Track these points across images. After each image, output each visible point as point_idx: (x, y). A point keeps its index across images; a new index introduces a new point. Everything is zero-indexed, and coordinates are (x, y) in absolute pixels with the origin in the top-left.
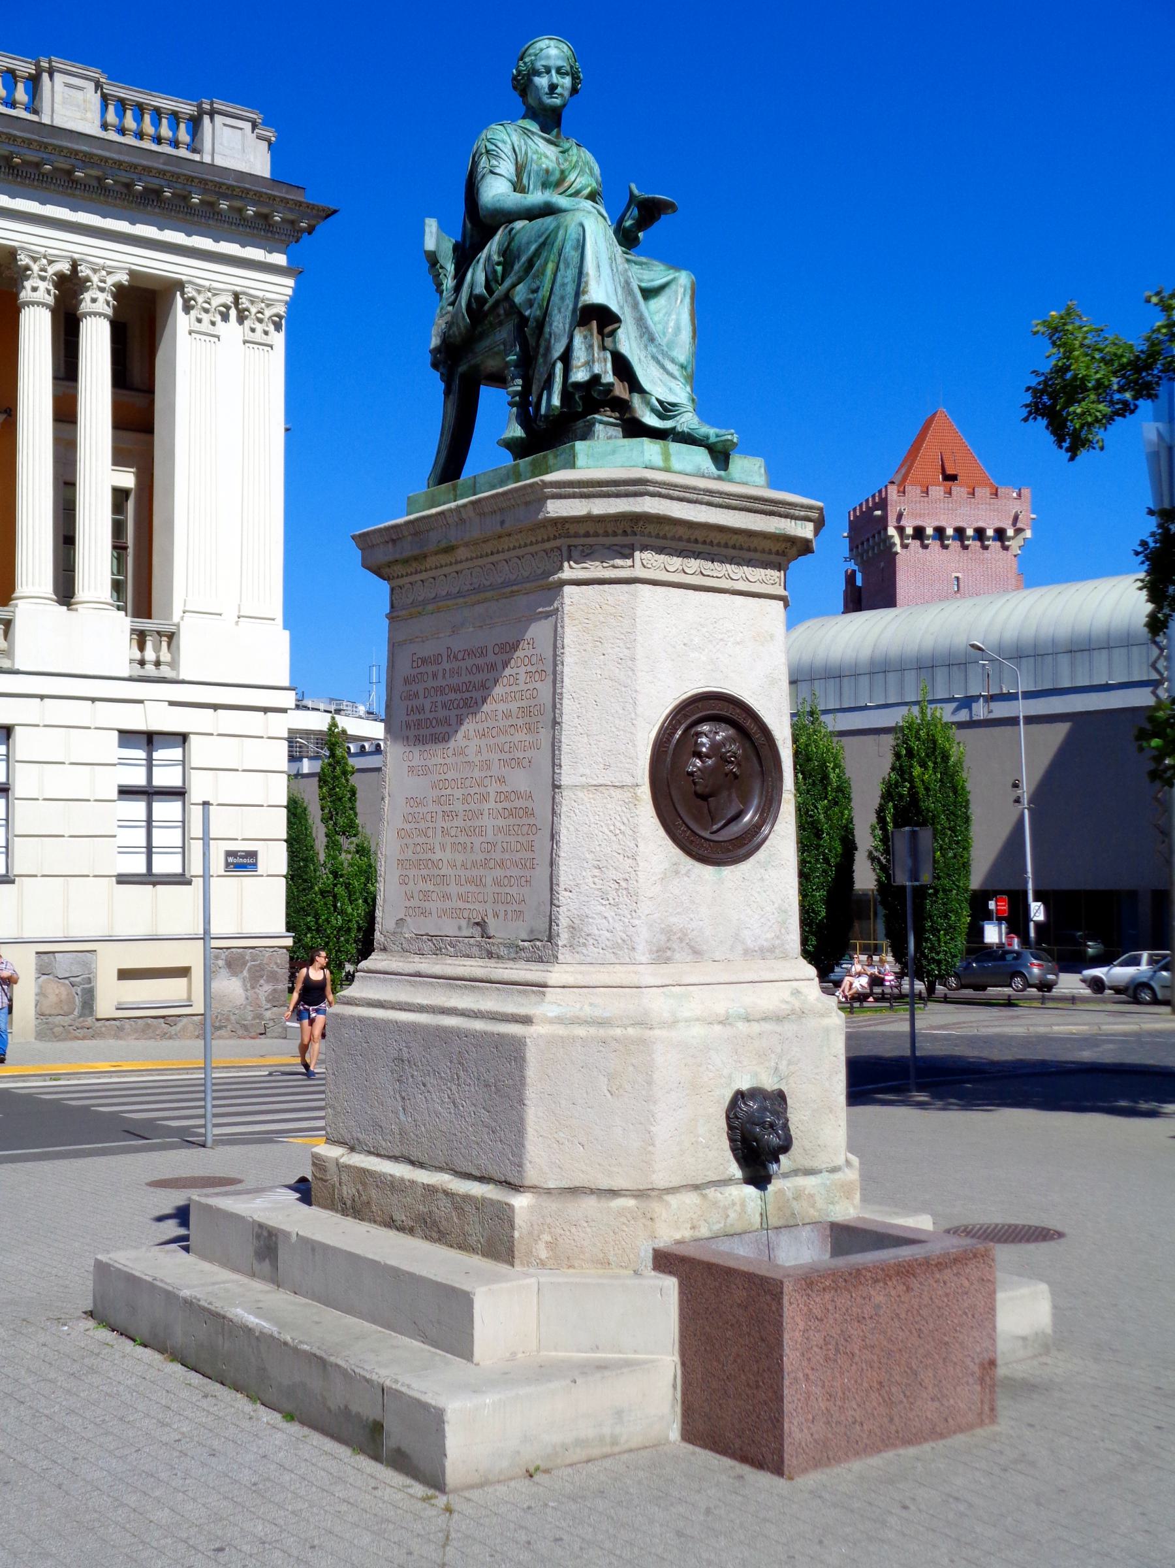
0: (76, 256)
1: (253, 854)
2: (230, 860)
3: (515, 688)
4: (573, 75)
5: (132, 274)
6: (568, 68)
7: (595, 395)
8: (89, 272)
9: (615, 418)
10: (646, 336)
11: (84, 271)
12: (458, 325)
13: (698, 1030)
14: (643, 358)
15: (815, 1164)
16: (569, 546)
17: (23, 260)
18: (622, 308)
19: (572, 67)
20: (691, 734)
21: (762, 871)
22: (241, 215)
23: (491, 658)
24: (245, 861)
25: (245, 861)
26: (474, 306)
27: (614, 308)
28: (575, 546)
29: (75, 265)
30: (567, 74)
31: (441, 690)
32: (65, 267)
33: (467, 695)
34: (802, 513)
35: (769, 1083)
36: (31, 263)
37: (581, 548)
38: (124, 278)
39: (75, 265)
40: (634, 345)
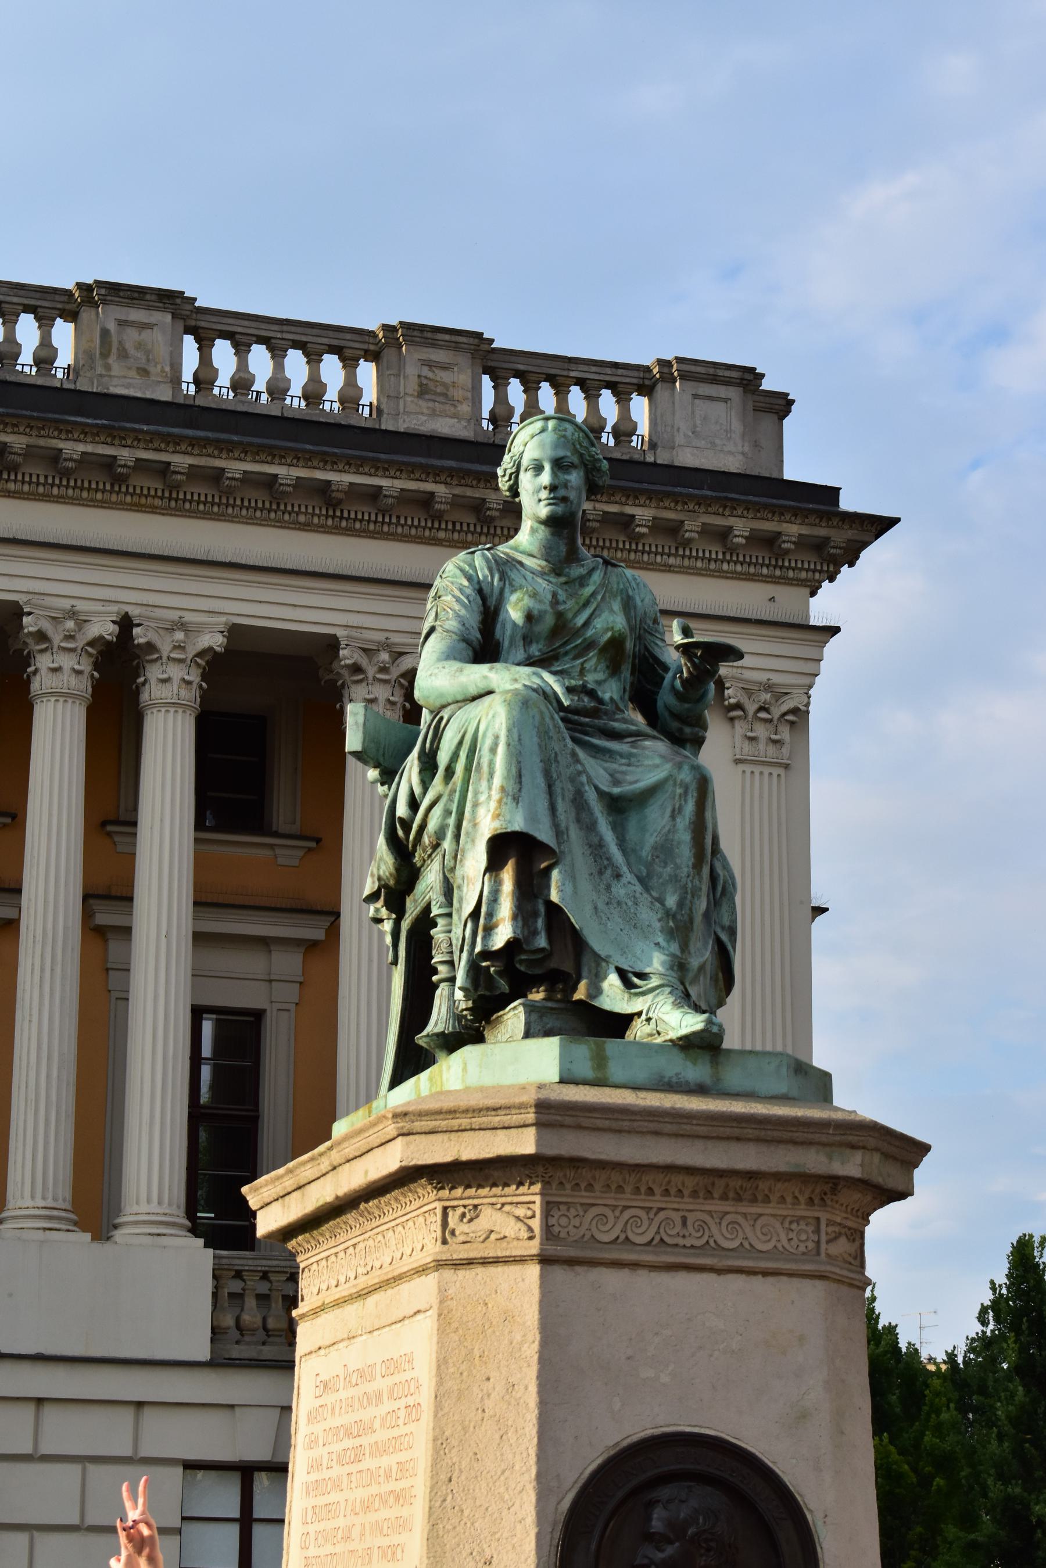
3: (396, 1432)
4: (585, 465)
6: (575, 460)
7: (522, 968)
9: (558, 1001)
10: (609, 872)
12: (386, 863)
14: (601, 905)
16: (445, 1209)
17: (347, 655)
18: (559, 833)
19: (581, 455)
22: (725, 546)
23: (381, 1384)
26: (400, 833)
27: (544, 834)
28: (454, 1207)
30: (573, 466)
31: (334, 1431)
33: (358, 1442)
34: (838, 1138)
36: (364, 662)
37: (462, 1209)
40: (585, 885)
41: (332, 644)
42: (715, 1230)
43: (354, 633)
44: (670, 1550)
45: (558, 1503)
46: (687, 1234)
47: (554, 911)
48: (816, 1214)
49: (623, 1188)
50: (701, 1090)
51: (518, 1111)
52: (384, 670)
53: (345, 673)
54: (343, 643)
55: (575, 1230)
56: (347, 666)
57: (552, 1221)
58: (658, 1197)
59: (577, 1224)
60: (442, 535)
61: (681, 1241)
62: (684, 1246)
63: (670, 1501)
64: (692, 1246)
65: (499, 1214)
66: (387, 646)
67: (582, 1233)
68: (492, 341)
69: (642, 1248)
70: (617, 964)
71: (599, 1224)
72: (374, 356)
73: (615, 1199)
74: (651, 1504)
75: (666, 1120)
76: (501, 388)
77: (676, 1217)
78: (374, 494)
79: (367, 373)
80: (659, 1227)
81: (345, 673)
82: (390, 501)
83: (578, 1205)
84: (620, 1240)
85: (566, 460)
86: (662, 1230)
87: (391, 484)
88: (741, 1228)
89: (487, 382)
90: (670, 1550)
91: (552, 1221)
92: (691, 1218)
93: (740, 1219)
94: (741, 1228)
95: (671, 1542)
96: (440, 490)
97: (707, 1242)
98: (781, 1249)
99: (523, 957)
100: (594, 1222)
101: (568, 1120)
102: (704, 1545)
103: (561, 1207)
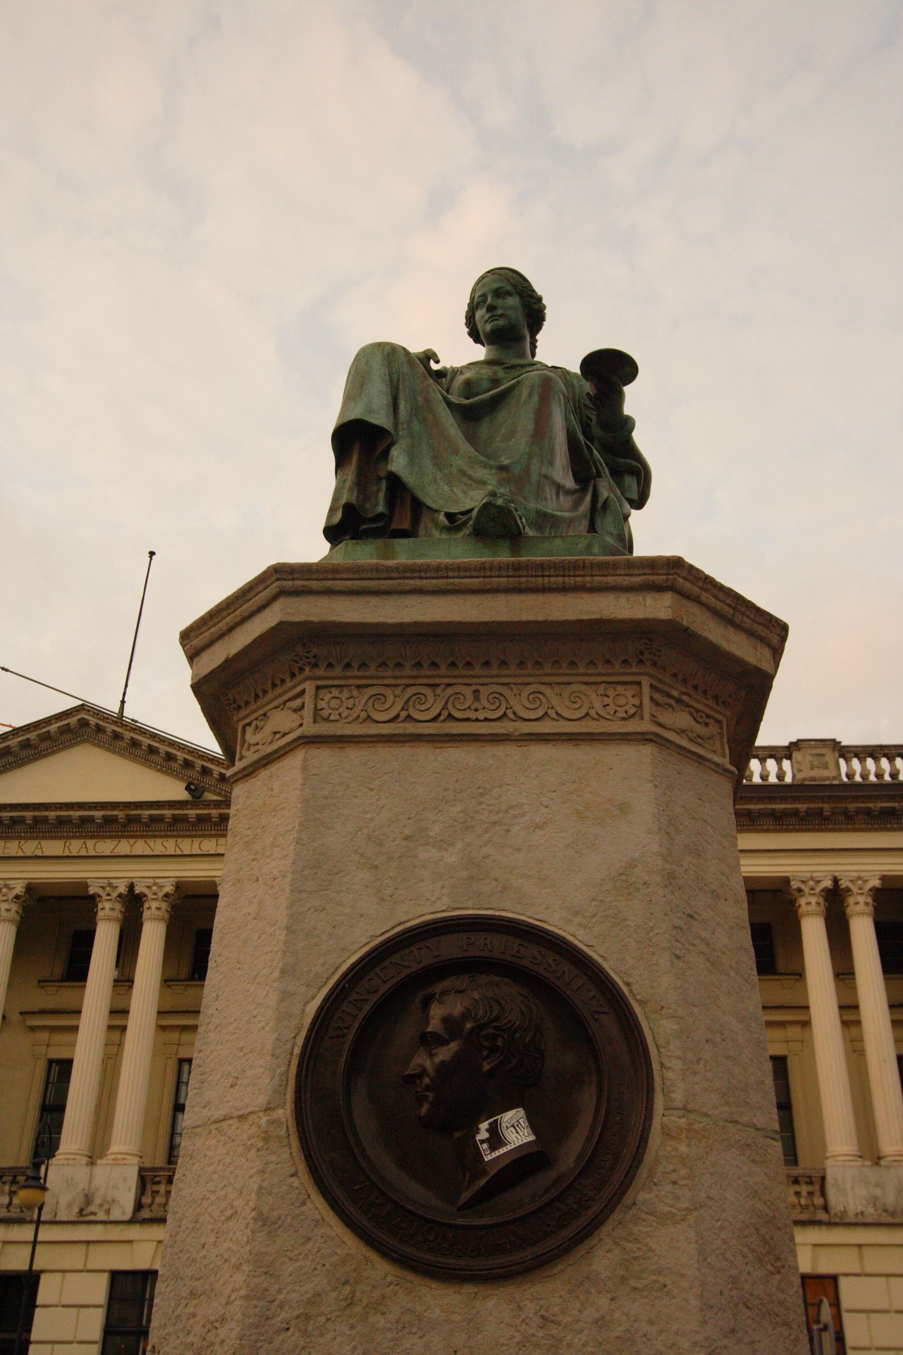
0: (837, 874)
5: (883, 878)
11: (844, 884)
17: (794, 884)
21: (603, 1301)
29: (836, 881)
30: (509, 294)
32: (828, 883)
36: (803, 886)
38: (876, 883)
39: (836, 881)
41: (786, 881)
42: (513, 702)
43: (795, 874)
44: (445, 1053)
45: (306, 1004)
46: (480, 707)
47: (395, 484)
48: (636, 679)
49: (402, 665)
51: (264, 586)
52: (812, 889)
53: (796, 893)
54: (791, 879)
55: (347, 712)
56: (795, 889)
57: (322, 704)
58: (443, 671)
59: (350, 706)
60: (830, 826)
61: (473, 715)
62: (477, 720)
63: (444, 993)
64: (486, 720)
65: (282, 712)
67: (356, 714)
68: (840, 743)
69: (428, 724)
70: (446, 510)
71: (375, 704)
72: (789, 757)
73: (396, 678)
74: (426, 1003)
75: (428, 575)
76: (849, 763)
77: (468, 692)
78: (796, 813)
79: (786, 764)
80: (447, 702)
81: (796, 893)
82: (803, 814)
83: (353, 687)
84: (401, 718)
85: (502, 289)
86: (450, 706)
87: (802, 807)
88: (546, 697)
89: (842, 762)
90: (445, 1053)
91: (322, 704)
92: (484, 691)
93: (543, 688)
94: (546, 697)
95: (444, 1042)
96: (826, 807)
97: (505, 714)
98: (596, 717)
99: (364, 527)
100: (370, 703)
101: (314, 585)
102: (486, 1044)
103: (333, 689)
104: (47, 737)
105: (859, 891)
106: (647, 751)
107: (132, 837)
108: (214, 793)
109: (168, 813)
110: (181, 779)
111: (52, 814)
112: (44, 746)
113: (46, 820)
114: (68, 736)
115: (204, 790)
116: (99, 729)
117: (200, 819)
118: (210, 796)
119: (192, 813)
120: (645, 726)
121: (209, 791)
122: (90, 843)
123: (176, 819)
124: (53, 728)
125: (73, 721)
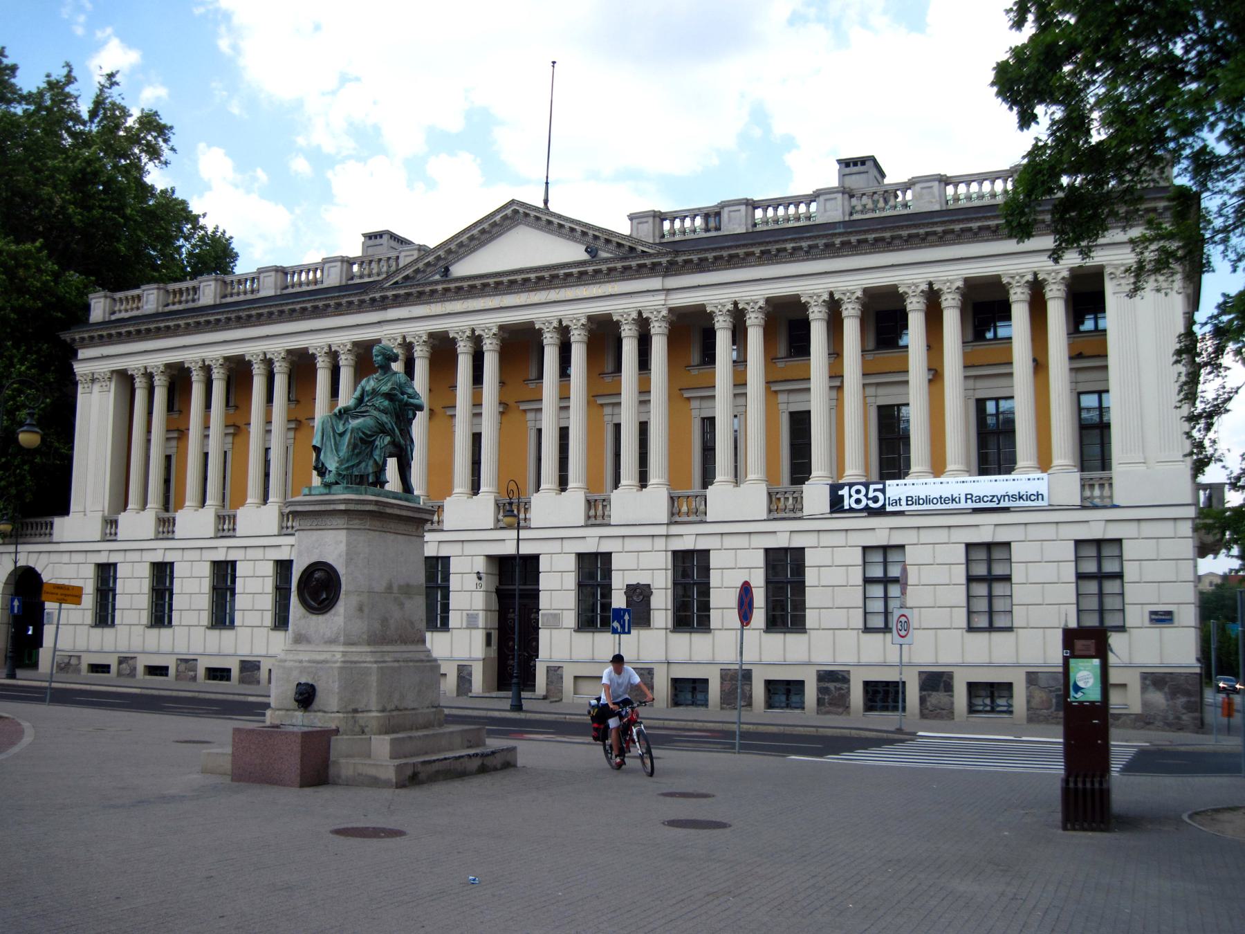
1: (1170, 613)
2: (1153, 617)
8: (1046, 276)
11: (1041, 277)
13: (291, 664)
15: (326, 710)
17: (1005, 280)
20: (313, 573)
24: (1163, 617)
25: (1163, 617)
32: (1029, 277)
35: (310, 682)
39: (1035, 274)
50: (327, 494)
66: (1018, 274)
104: (495, 225)
105: (1054, 281)
106: (345, 531)
107: (556, 288)
108: (605, 251)
109: (575, 270)
110: (583, 244)
111: (505, 279)
112: (494, 230)
113: (501, 283)
114: (508, 222)
115: (597, 250)
116: (526, 215)
117: (597, 272)
118: (603, 255)
119: (590, 269)
120: (345, 526)
121: (601, 250)
122: (532, 294)
123: (582, 274)
124: (498, 218)
125: (509, 211)
